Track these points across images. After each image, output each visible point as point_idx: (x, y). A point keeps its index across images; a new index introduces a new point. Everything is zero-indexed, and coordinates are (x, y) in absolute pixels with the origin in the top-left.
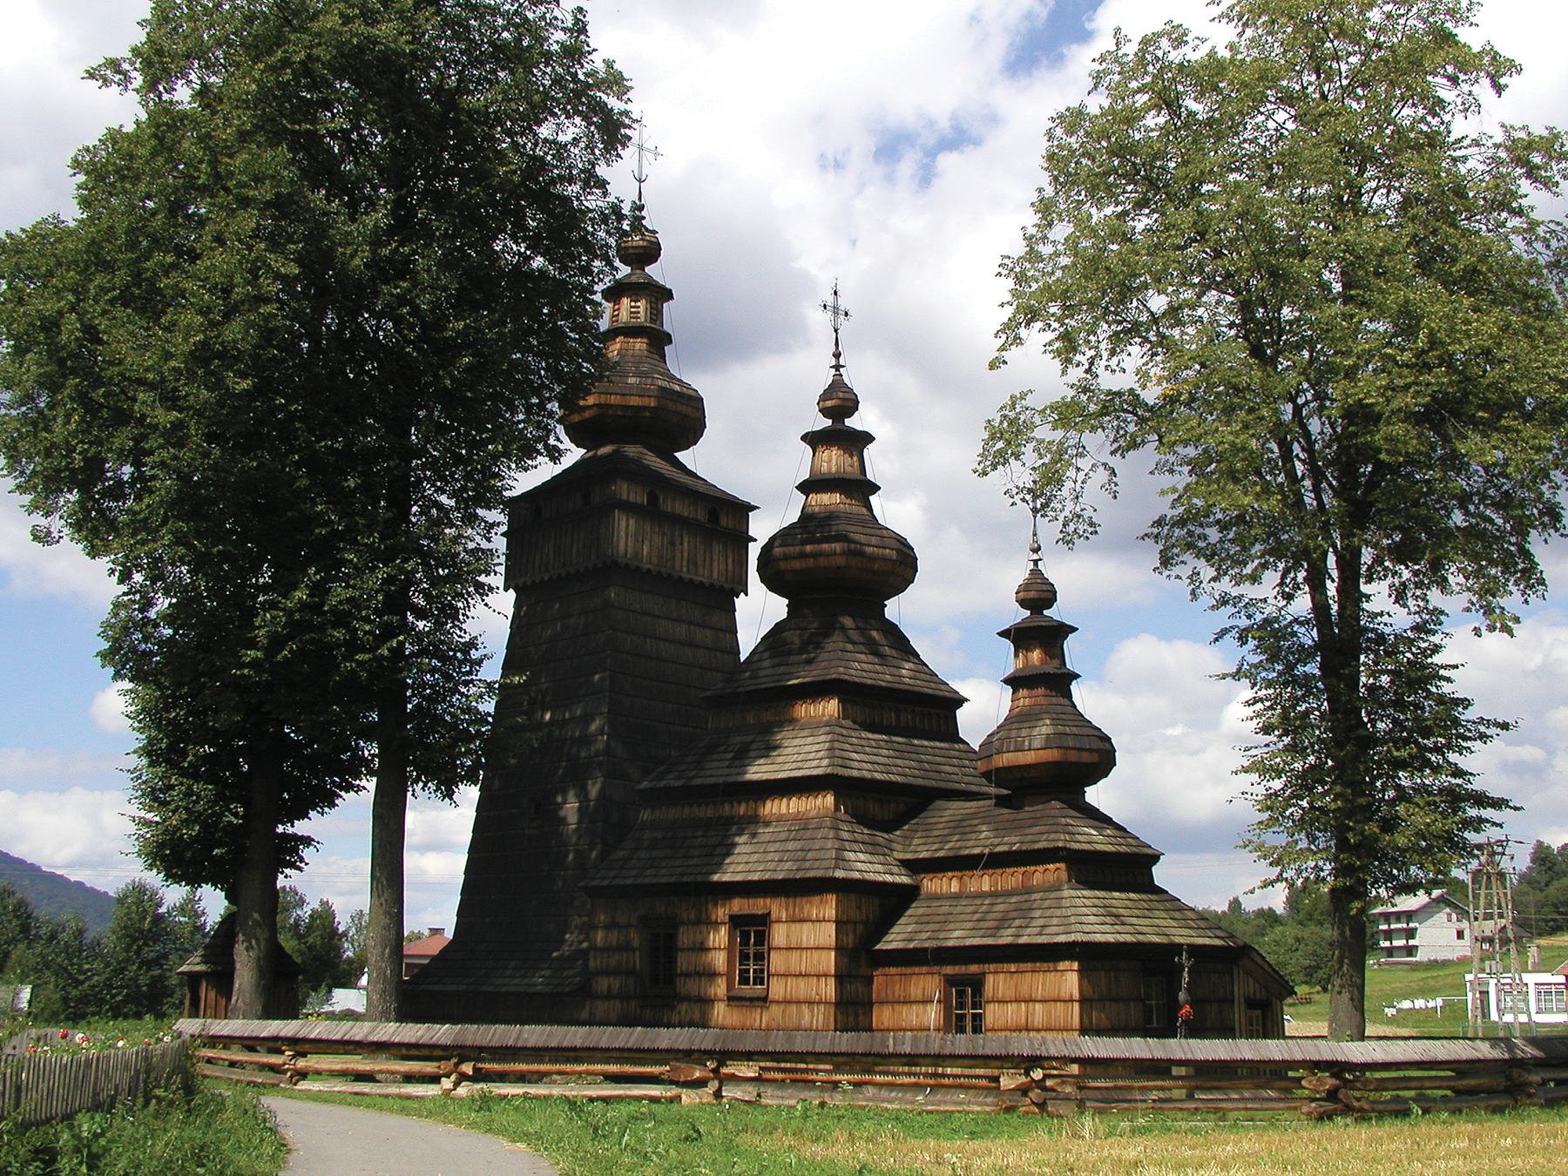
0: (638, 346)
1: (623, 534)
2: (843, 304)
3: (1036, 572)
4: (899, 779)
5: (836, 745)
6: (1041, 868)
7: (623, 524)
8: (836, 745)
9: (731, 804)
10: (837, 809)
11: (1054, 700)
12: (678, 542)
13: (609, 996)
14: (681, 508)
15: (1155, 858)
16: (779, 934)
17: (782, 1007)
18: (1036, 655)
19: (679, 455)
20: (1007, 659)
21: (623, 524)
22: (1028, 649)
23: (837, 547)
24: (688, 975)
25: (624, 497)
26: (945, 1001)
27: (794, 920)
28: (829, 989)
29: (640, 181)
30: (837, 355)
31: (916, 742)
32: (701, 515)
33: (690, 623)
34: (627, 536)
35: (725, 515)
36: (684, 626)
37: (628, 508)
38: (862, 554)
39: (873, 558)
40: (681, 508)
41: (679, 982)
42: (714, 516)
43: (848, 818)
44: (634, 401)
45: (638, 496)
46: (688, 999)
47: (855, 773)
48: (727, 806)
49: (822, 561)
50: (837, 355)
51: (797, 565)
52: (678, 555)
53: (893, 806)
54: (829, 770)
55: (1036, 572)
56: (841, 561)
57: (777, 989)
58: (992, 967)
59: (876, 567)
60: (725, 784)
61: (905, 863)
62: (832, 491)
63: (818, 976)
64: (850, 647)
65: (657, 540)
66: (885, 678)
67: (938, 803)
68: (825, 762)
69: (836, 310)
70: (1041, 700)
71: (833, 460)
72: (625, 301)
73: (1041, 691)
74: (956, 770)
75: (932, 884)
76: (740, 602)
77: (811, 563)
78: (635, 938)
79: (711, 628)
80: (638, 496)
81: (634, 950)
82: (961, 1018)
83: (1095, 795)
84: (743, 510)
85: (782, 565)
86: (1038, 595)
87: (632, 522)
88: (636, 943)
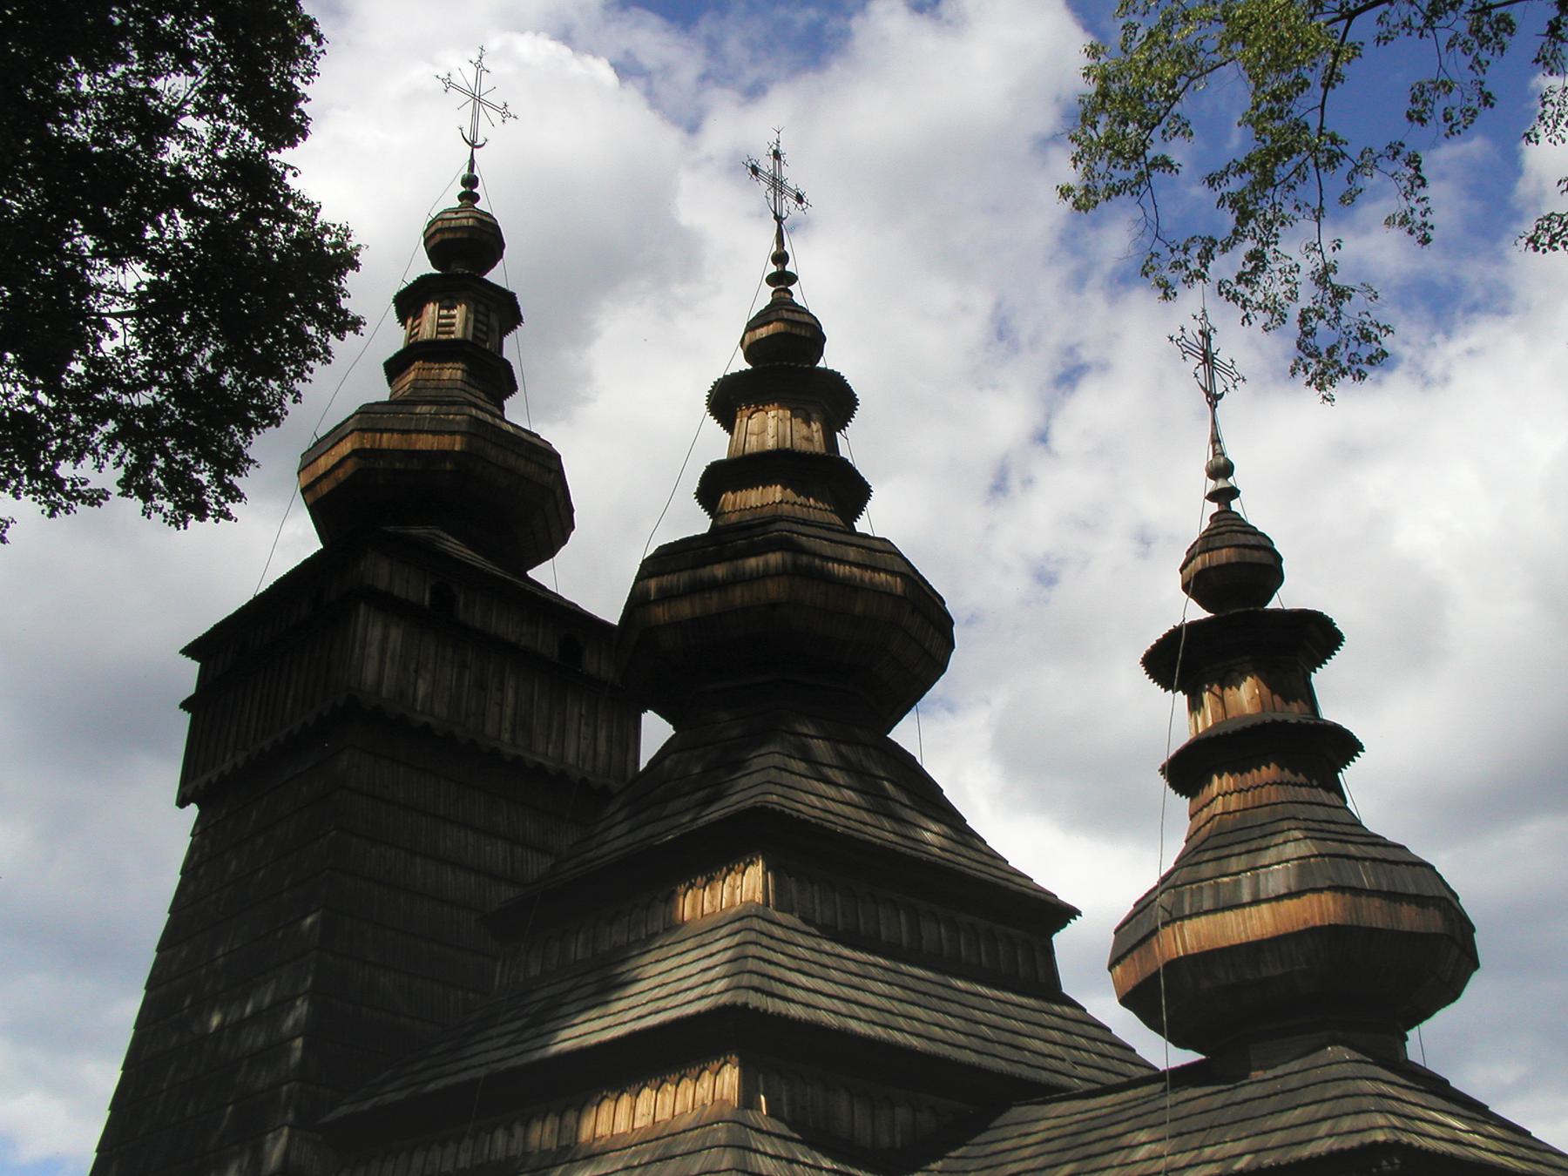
0: (446, 374)
1: (373, 650)
2: (792, 176)
4: (915, 1042)
5: (752, 950)
7: (376, 633)
8: (752, 950)
9: (509, 1130)
10: (747, 1099)
11: (1304, 793)
14: (506, 626)
18: (1246, 696)
19: (530, 573)
21: (376, 633)
22: (1229, 679)
23: (775, 558)
25: (382, 584)
29: (473, 145)
30: (780, 258)
31: (960, 984)
37: (390, 606)
38: (829, 579)
39: (847, 584)
40: (506, 626)
43: (783, 1129)
44: (425, 442)
45: (415, 589)
47: (796, 1011)
48: (500, 1137)
49: (738, 595)
50: (780, 258)
51: (685, 609)
53: (902, 1114)
54: (725, 999)
56: (774, 590)
59: (859, 608)
62: (767, 483)
64: (801, 766)
66: (882, 832)
67: (1017, 1113)
68: (720, 985)
69: (777, 184)
70: (1273, 794)
71: (768, 427)
72: (431, 309)
73: (1268, 772)
74: (1058, 1051)
77: (714, 602)
80: (415, 589)
87: (396, 634)
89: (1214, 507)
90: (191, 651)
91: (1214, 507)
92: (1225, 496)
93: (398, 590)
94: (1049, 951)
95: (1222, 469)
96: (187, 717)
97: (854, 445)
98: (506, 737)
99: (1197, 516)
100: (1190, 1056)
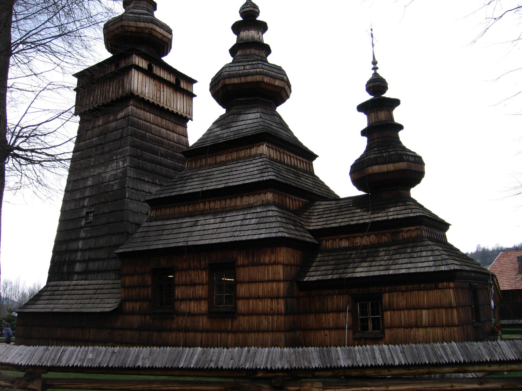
3: (375, 74)
6: (405, 229)
7: (136, 76)
12: (162, 90)
13: (133, 313)
15: (445, 226)
16: (243, 273)
17: (246, 318)
20: (362, 121)
21: (136, 76)
24: (182, 300)
25: (137, 64)
26: (353, 312)
27: (254, 265)
28: (281, 305)
32: (172, 79)
33: (167, 129)
34: (139, 83)
35: (182, 84)
36: (165, 130)
37: (139, 69)
41: (177, 304)
42: (178, 82)
46: (183, 314)
52: (162, 96)
55: (375, 74)
57: (242, 306)
58: (387, 288)
60: (203, 192)
61: (311, 232)
63: (272, 298)
65: (151, 86)
75: (328, 244)
76: (189, 124)
77: (243, 80)
78: (149, 280)
79: (176, 133)
80: (143, 64)
81: (148, 286)
82: (364, 321)
83: (415, 193)
84: (192, 81)
85: (228, 81)
86: (377, 85)
88: (150, 283)
89: (373, 72)
90: (76, 75)
91: (373, 72)
92: (375, 69)
93: (140, 65)
94: (312, 165)
95: (374, 63)
96: (75, 93)
97: (267, 38)
98: (165, 103)
99: (369, 75)
100: (362, 193)
